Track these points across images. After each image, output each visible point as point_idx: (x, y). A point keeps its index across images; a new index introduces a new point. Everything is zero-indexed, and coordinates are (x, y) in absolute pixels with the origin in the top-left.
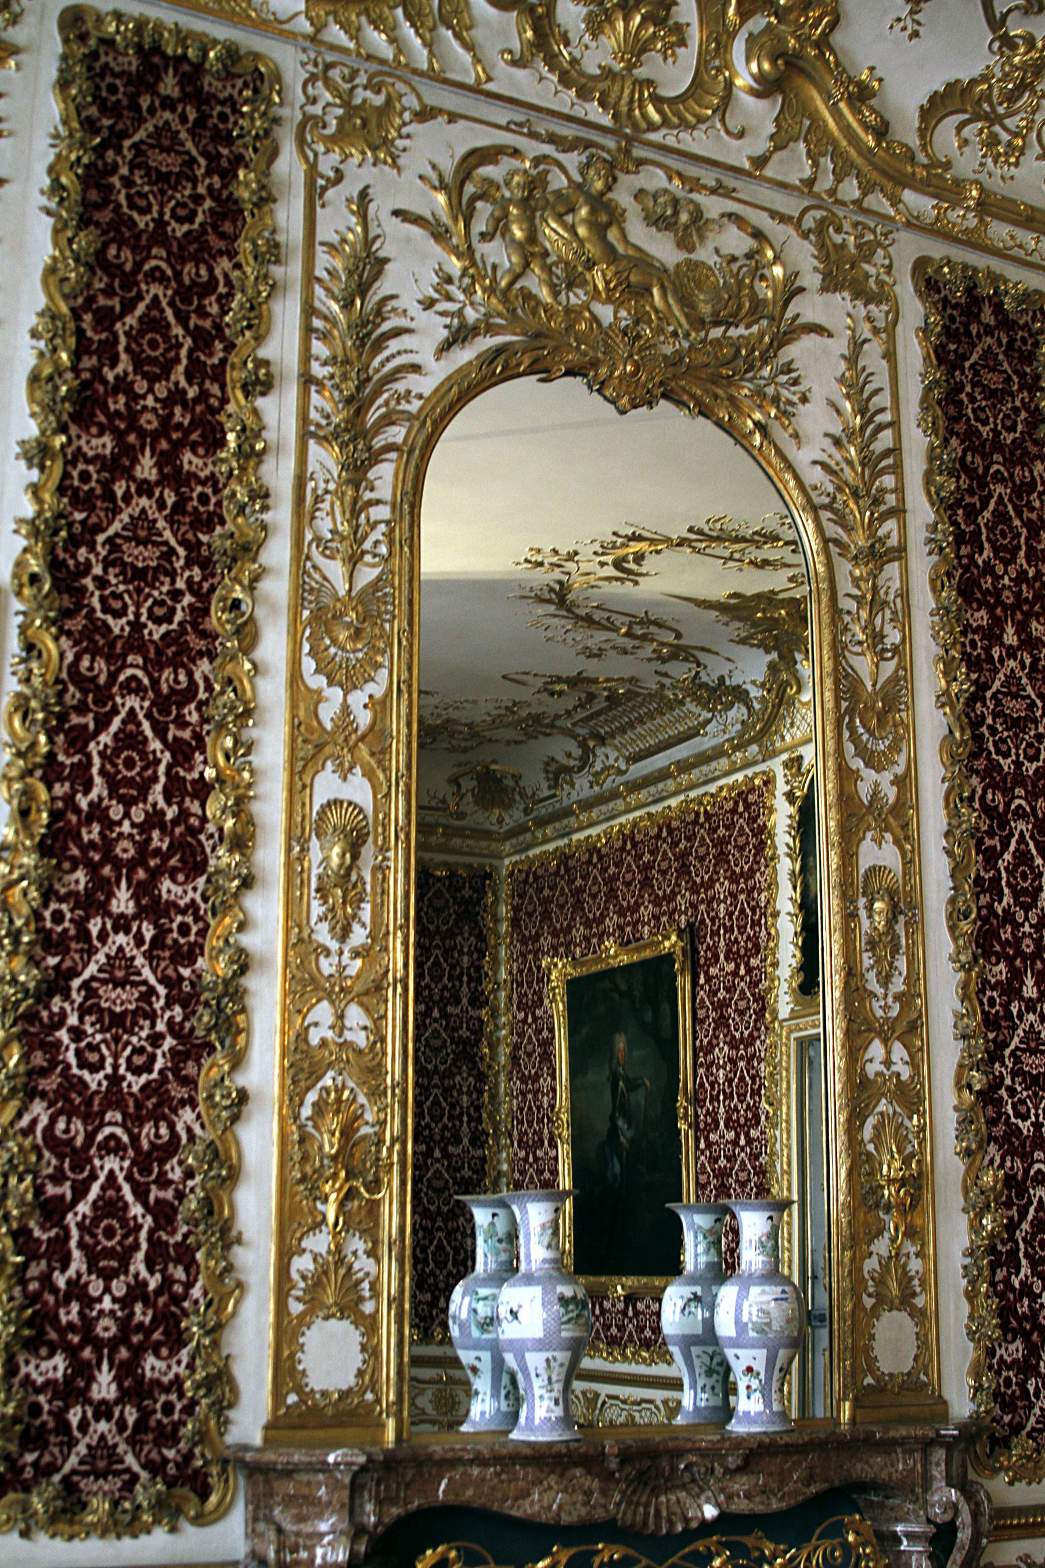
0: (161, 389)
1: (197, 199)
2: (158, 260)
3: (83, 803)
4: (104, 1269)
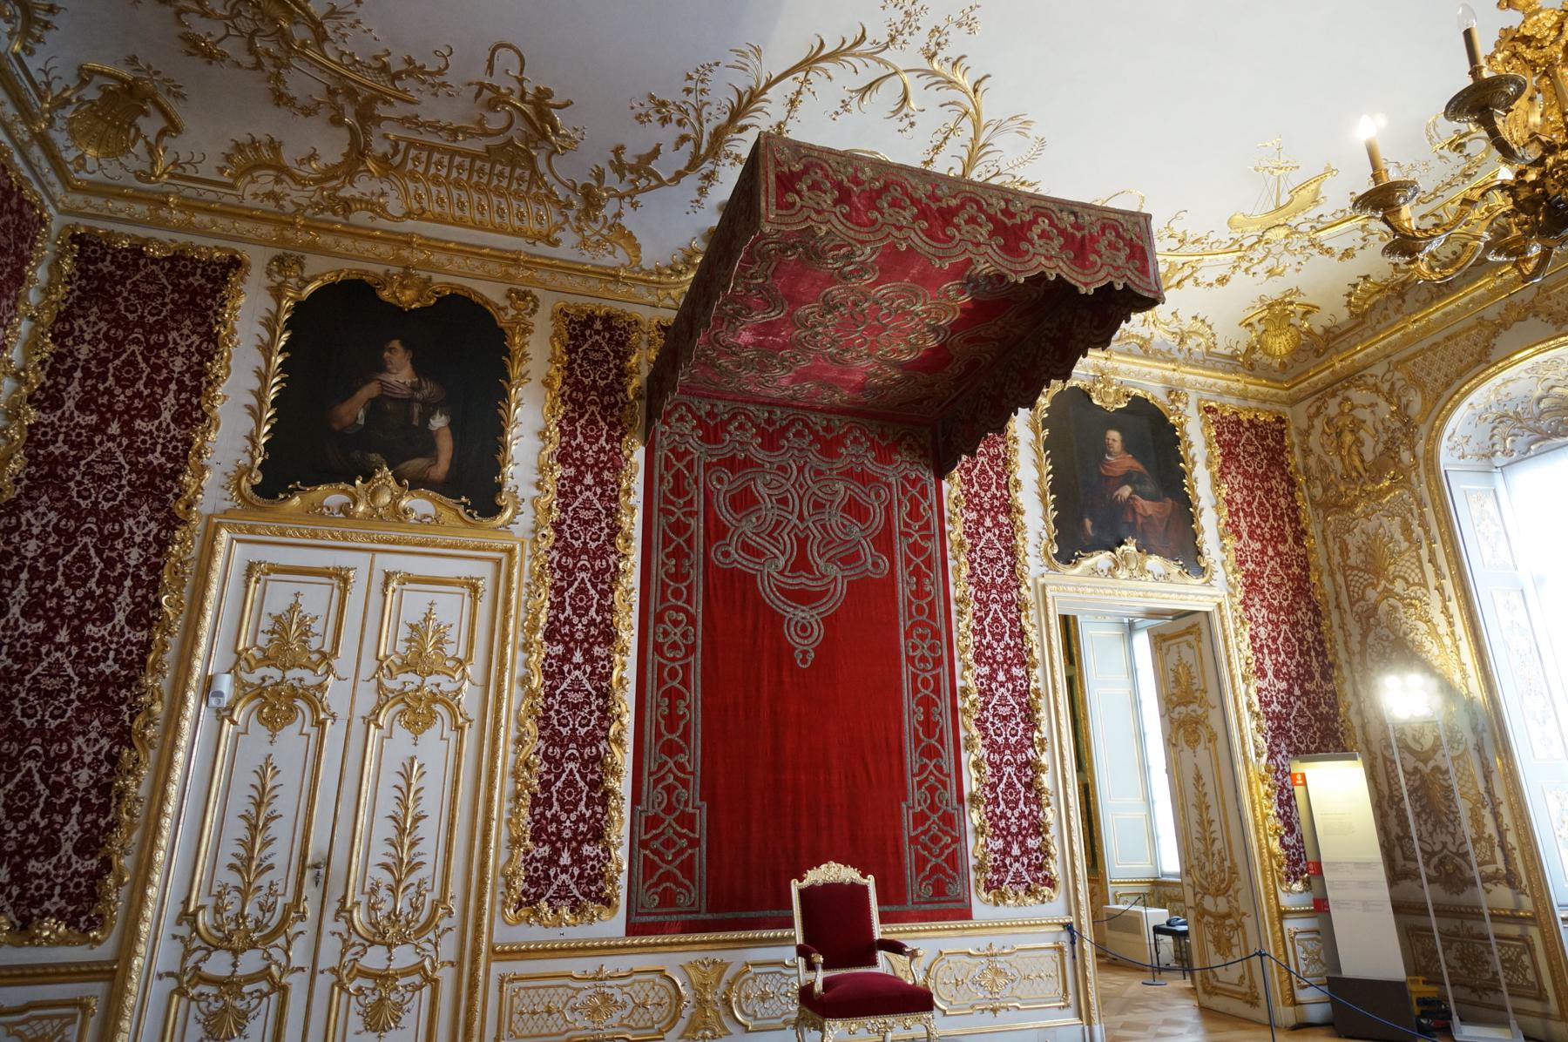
0: (595, 448)
1: (610, 370)
2: (593, 396)
3: (562, 617)
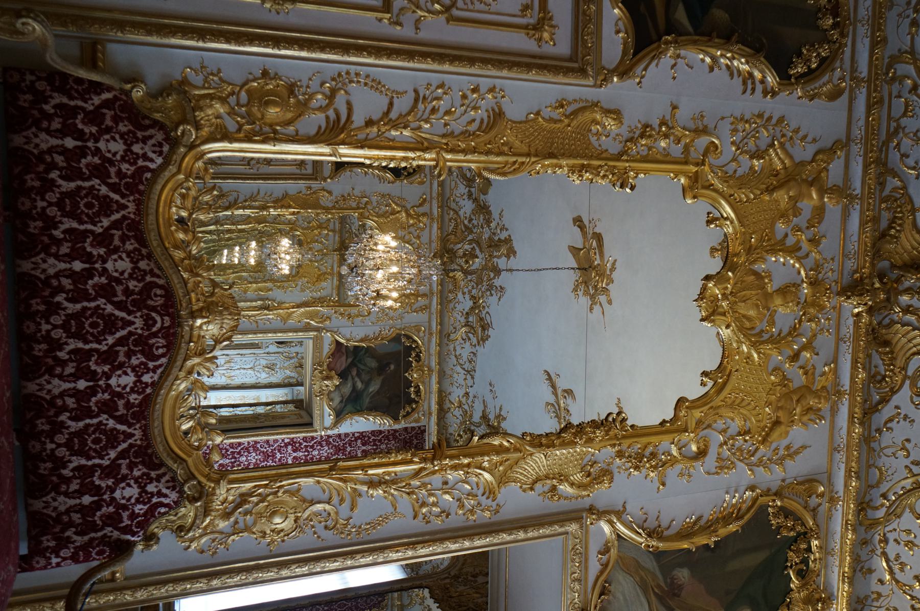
4: (70, 323)
